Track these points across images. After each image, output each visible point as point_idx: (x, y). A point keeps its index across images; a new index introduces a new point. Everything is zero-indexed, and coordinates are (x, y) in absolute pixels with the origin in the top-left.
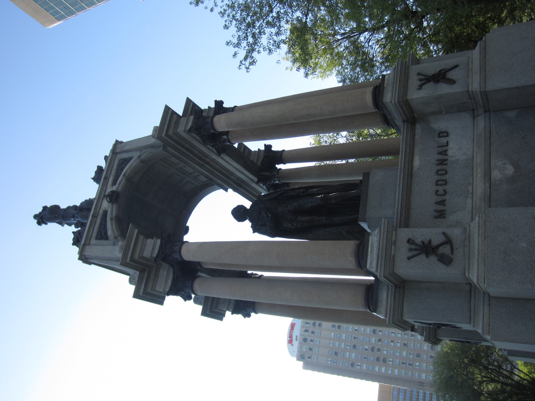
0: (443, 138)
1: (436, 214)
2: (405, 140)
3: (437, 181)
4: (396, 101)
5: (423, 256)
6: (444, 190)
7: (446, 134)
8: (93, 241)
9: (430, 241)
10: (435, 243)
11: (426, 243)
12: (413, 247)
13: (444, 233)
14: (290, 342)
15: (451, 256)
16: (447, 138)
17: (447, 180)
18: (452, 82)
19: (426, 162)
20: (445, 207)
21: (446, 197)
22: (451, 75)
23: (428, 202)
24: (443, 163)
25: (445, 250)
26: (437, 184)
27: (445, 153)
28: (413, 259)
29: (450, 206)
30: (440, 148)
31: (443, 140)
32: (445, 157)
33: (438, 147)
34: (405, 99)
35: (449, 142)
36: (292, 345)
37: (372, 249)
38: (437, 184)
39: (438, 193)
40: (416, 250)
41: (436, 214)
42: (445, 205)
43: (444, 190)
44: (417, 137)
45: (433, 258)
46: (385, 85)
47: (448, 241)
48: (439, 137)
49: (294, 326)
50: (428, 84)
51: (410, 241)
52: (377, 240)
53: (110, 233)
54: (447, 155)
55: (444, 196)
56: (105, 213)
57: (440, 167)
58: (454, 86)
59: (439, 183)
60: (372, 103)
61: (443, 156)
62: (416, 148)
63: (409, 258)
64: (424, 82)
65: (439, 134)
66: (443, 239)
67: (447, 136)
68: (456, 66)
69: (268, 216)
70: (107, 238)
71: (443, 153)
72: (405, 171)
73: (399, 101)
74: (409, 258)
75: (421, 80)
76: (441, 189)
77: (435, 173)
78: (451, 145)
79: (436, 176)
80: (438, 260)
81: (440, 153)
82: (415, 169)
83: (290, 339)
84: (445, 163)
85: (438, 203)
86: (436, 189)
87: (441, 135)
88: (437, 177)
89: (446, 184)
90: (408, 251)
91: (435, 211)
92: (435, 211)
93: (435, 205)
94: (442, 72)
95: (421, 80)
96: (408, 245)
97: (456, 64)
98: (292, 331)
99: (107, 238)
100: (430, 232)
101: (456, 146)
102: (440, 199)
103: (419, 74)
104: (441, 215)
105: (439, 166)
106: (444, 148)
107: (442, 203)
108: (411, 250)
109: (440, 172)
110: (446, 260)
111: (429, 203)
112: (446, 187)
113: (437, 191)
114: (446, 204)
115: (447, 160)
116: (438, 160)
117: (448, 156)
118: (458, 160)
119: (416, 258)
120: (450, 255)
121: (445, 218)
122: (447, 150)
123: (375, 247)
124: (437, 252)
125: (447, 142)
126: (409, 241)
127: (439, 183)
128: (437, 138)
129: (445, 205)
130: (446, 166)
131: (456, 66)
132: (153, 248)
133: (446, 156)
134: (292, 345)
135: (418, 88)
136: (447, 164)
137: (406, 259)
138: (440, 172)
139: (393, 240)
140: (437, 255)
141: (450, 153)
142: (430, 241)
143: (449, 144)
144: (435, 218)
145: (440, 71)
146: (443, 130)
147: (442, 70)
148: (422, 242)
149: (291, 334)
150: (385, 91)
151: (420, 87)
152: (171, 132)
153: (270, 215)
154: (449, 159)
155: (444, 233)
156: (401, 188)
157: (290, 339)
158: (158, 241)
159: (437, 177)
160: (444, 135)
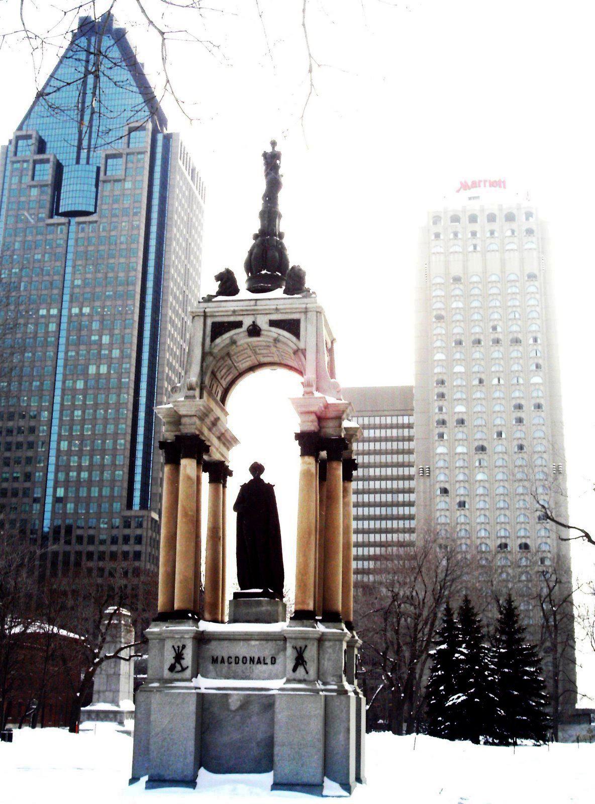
1: (215, 658)
3: (238, 657)
5: (174, 655)
7: (273, 662)
8: (209, 322)
9: (184, 659)
12: (181, 649)
13: (188, 667)
14: (465, 186)
18: (294, 670)
21: (226, 664)
22: (301, 670)
25: (178, 668)
26: (236, 657)
27: (259, 662)
31: (268, 661)
32: (256, 662)
36: (458, 191)
38: (236, 657)
39: (230, 659)
40: (179, 650)
41: (215, 658)
45: (173, 661)
47: (184, 669)
48: (272, 658)
49: (500, 187)
53: (218, 341)
56: (239, 324)
58: (291, 672)
63: (173, 647)
64: (299, 649)
65: (275, 658)
66: (184, 666)
67: (272, 663)
68: (307, 673)
70: (213, 339)
74: (173, 647)
75: (301, 648)
76: (233, 660)
78: (265, 666)
80: (172, 665)
81: (259, 659)
82: (249, 642)
83: (470, 184)
84: (252, 663)
85: (223, 658)
87: (273, 659)
91: (217, 657)
92: (217, 657)
95: (301, 648)
98: (487, 184)
99: (213, 339)
103: (306, 646)
104: (215, 661)
107: (223, 661)
108: (178, 647)
110: (172, 668)
112: (233, 664)
113: (231, 657)
115: (253, 663)
116: (254, 658)
125: (267, 664)
126: (184, 647)
131: (307, 673)
134: (458, 191)
140: (175, 663)
141: (259, 666)
142: (184, 659)
145: (306, 662)
146: (277, 661)
149: (482, 184)
151: (295, 648)
155: (188, 667)
157: (470, 184)
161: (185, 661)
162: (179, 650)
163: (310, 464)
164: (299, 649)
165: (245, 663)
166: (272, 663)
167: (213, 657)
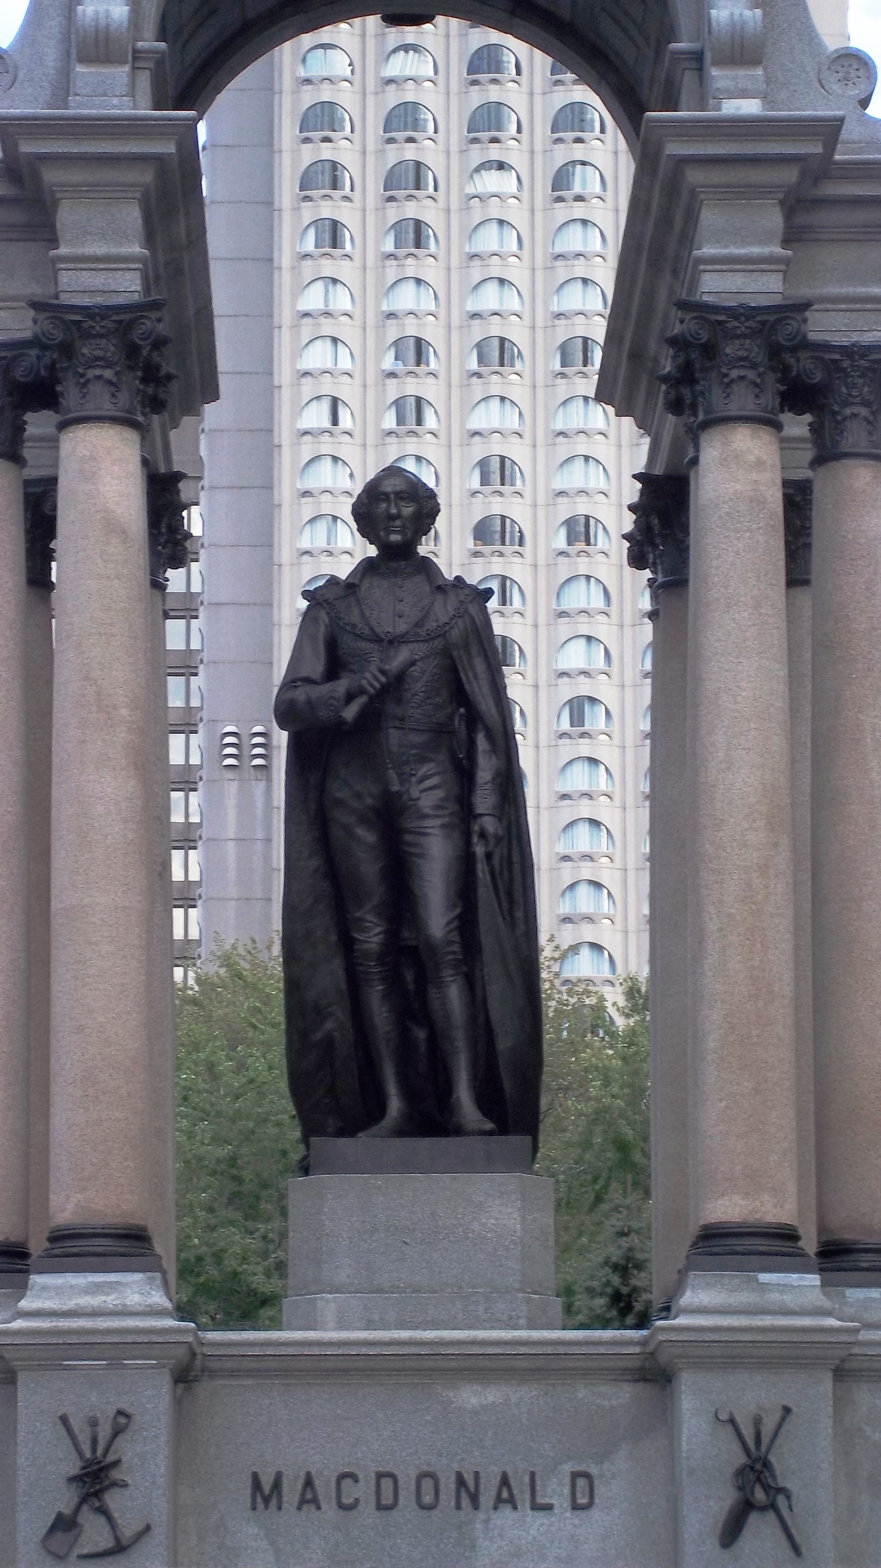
0: (567, 1491)
2: (561, 1350)
4: (661, 1337)
5: (74, 1467)
6: (357, 1501)
9: (125, 1485)
10: (113, 1500)
11: (115, 1475)
12: (104, 1434)
13: (148, 1528)
15: (76, 1554)
16: (567, 1504)
17: (395, 1513)
19: (474, 1431)
20: (293, 1509)
23: (312, 1448)
24: (464, 1495)
26: (380, 1476)
28: (63, 1432)
29: (298, 1525)
30: (527, 1479)
32: (487, 1498)
33: (533, 1475)
34: (681, 1366)
35: (548, 1512)
37: (97, 1289)
38: (380, 1476)
39: (347, 1483)
40: (94, 1441)
42: (299, 1508)
43: (357, 1501)
44: (582, 1392)
46: (765, 1277)
47: (119, 1549)
48: (575, 1476)
50: (736, 1447)
51: (122, 1420)
52: (125, 1306)
54: (495, 1508)
55: (334, 1502)
57: (448, 1485)
58: (712, 1544)
59: (387, 1484)
60: (713, 1221)
61: (493, 1492)
62: (534, 1393)
63: (64, 1420)
64: (748, 1433)
65: (587, 1476)
66: (129, 1528)
68: (796, 1549)
69: (350, 697)
71: (505, 1494)
72: (430, 1359)
73: (666, 1344)
74: (64, 1420)
75: (757, 1422)
76: (364, 1490)
77: (425, 1468)
78: (537, 1522)
79: (413, 1473)
80: (60, 1517)
81: (505, 1481)
84: (465, 1501)
85: (309, 1482)
86: (361, 1476)
88: (407, 1477)
89: (380, 1507)
90: (91, 1414)
93: (302, 1474)
94: (781, 1501)
95: (757, 1422)
96: (111, 1413)
97: (803, 1549)
100: (154, 1483)
101: (530, 1538)
102: (325, 1488)
105: (453, 1479)
106: (523, 1497)
108: (94, 1423)
109: (427, 1484)
111: (311, 1452)
112: (367, 1511)
113: (355, 1478)
114: (305, 1507)
116: (477, 1474)
117: (491, 1512)
118: (474, 1547)
119: (68, 1441)
120: (77, 1551)
121: (254, 1508)
122: (515, 1508)
123: (104, 1298)
124: (85, 1508)
125: (549, 1507)
127: (387, 1484)
128: (568, 1468)
129: (299, 1508)
130: (453, 1504)
131: (796, 1549)
132: (96, 259)
133: (491, 1503)
135: (724, 1416)
136: (458, 1507)
137: (62, 1411)
138: (427, 1484)
139: (126, 1362)
140: (78, 1509)
141: (506, 1517)
143: (541, 1513)
144: (255, 1477)
146: (600, 1490)
147: (788, 1497)
148: (117, 1463)
150: (734, 1278)
152: (694, 176)
153: (350, 713)
154: (481, 1515)
155: (148, 1528)
156: (364, 1351)
158: (129, 275)
159: (407, 1477)
160: (579, 1495)
161: (127, 1492)
162: (94, 1441)
163: (759, 464)
164: (748, 1433)
165: (430, 1508)
166: (576, 1507)
167: (255, 1477)
